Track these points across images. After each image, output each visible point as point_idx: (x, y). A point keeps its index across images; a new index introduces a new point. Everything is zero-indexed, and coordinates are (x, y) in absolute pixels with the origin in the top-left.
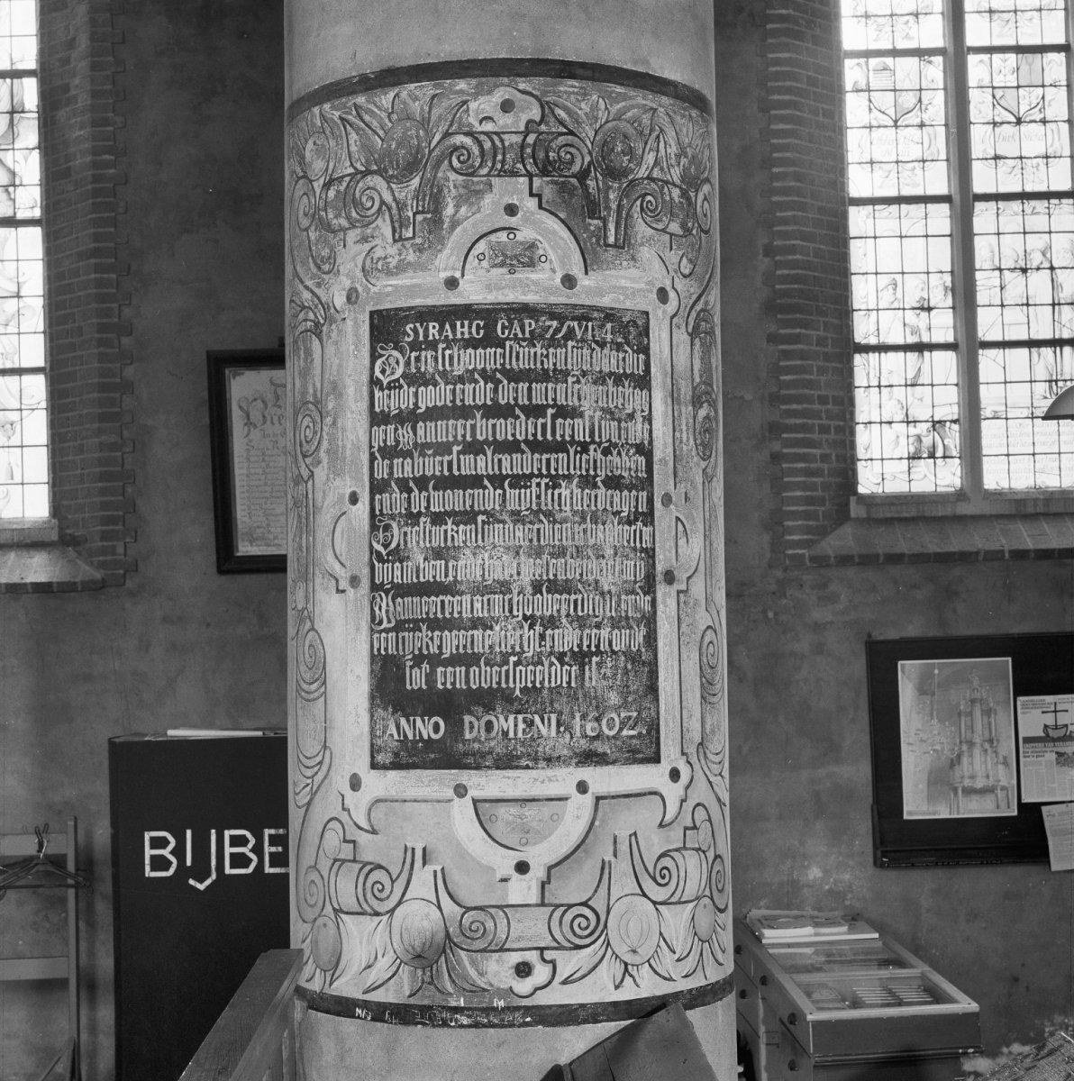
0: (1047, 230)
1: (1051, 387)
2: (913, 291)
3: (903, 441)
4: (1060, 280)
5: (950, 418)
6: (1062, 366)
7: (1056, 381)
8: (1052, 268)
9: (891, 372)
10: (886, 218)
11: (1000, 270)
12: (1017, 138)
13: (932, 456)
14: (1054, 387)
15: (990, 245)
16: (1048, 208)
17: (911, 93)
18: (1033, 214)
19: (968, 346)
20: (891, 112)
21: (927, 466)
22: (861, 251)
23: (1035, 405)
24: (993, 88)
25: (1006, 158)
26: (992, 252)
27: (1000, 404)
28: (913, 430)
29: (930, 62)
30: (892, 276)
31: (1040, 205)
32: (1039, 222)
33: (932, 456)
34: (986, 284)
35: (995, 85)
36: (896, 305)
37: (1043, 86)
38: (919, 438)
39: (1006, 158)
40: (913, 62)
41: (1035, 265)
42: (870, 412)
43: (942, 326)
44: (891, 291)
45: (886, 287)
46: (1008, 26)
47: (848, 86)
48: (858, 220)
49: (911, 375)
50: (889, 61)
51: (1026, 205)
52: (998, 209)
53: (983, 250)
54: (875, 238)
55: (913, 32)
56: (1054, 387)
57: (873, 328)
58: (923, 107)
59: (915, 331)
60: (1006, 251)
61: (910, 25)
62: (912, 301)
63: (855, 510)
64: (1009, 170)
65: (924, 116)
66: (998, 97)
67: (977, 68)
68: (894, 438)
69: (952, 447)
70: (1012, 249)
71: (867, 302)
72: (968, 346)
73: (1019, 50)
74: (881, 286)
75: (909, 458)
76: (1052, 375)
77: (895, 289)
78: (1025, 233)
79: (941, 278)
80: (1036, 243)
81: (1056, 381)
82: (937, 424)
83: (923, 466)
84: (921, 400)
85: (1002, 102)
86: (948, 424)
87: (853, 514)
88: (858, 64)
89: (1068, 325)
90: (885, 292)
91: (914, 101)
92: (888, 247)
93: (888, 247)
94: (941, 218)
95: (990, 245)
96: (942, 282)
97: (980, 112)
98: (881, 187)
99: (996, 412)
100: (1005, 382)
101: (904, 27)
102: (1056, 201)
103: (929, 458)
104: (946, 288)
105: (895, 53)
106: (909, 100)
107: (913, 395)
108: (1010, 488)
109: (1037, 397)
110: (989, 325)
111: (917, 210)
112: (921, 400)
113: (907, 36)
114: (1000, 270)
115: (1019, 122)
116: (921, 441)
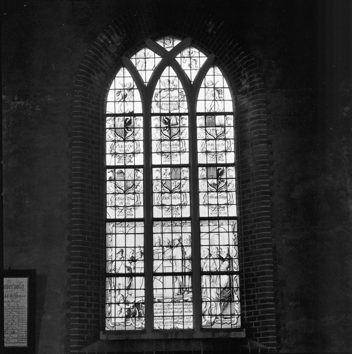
0: (181, 232)
1: (180, 291)
2: (129, 254)
3: (123, 310)
4: (185, 250)
5: (142, 302)
6: (185, 282)
7: (183, 288)
8: (182, 246)
9: (120, 284)
11: (163, 246)
12: (170, 198)
13: (134, 316)
14: (182, 291)
15: (159, 237)
16: (181, 224)
17: (131, 182)
18: (175, 226)
19: (149, 274)
20: (123, 188)
21: (132, 320)
22: (110, 239)
23: (174, 297)
24: (162, 180)
25: (166, 205)
26: (160, 240)
27: (161, 297)
28: (127, 307)
29: (139, 171)
31: (178, 223)
32: (178, 229)
33: (134, 316)
34: (157, 251)
35: (162, 179)
36: (122, 259)
37: (180, 179)
38: (129, 309)
39: (166, 205)
40: (132, 170)
41: (176, 244)
42: (111, 299)
43: (140, 267)
44: (121, 254)
45: (119, 252)
46: (168, 158)
47: (108, 179)
48: (110, 228)
49: (127, 285)
50: (123, 170)
51: (173, 223)
52: (162, 224)
53: (156, 238)
54: (116, 234)
55: (133, 160)
56: (182, 291)
57: (113, 268)
58: (135, 186)
59: (129, 269)
60: (165, 239)
61: (131, 157)
62: (128, 257)
63: (103, 337)
64: (167, 210)
65: (135, 190)
66: (163, 183)
67: (156, 173)
68: (120, 309)
69: (142, 313)
70: (167, 238)
72: (149, 274)
73: (172, 166)
74: (117, 252)
75: (125, 317)
76: (181, 286)
77: (122, 253)
78: (172, 233)
79: (140, 249)
80: (176, 236)
81: (183, 288)
82: (136, 305)
83: (130, 321)
84: (131, 295)
85: (165, 185)
86: (141, 304)
87: (101, 339)
88: (111, 171)
89: (188, 267)
90: (119, 254)
91: (132, 184)
94: (140, 228)
95: (159, 237)
96: (140, 251)
97: (157, 189)
98: (118, 215)
99: (159, 300)
100: (163, 289)
101: (129, 158)
102: (184, 221)
103: (133, 317)
104: (142, 253)
105: (125, 167)
106: (130, 184)
107: (128, 293)
108: (164, 329)
109: (175, 294)
110: (157, 266)
111: (132, 224)
112: (131, 295)
113: (130, 161)
114: (163, 246)
115: (171, 192)
116: (130, 311)
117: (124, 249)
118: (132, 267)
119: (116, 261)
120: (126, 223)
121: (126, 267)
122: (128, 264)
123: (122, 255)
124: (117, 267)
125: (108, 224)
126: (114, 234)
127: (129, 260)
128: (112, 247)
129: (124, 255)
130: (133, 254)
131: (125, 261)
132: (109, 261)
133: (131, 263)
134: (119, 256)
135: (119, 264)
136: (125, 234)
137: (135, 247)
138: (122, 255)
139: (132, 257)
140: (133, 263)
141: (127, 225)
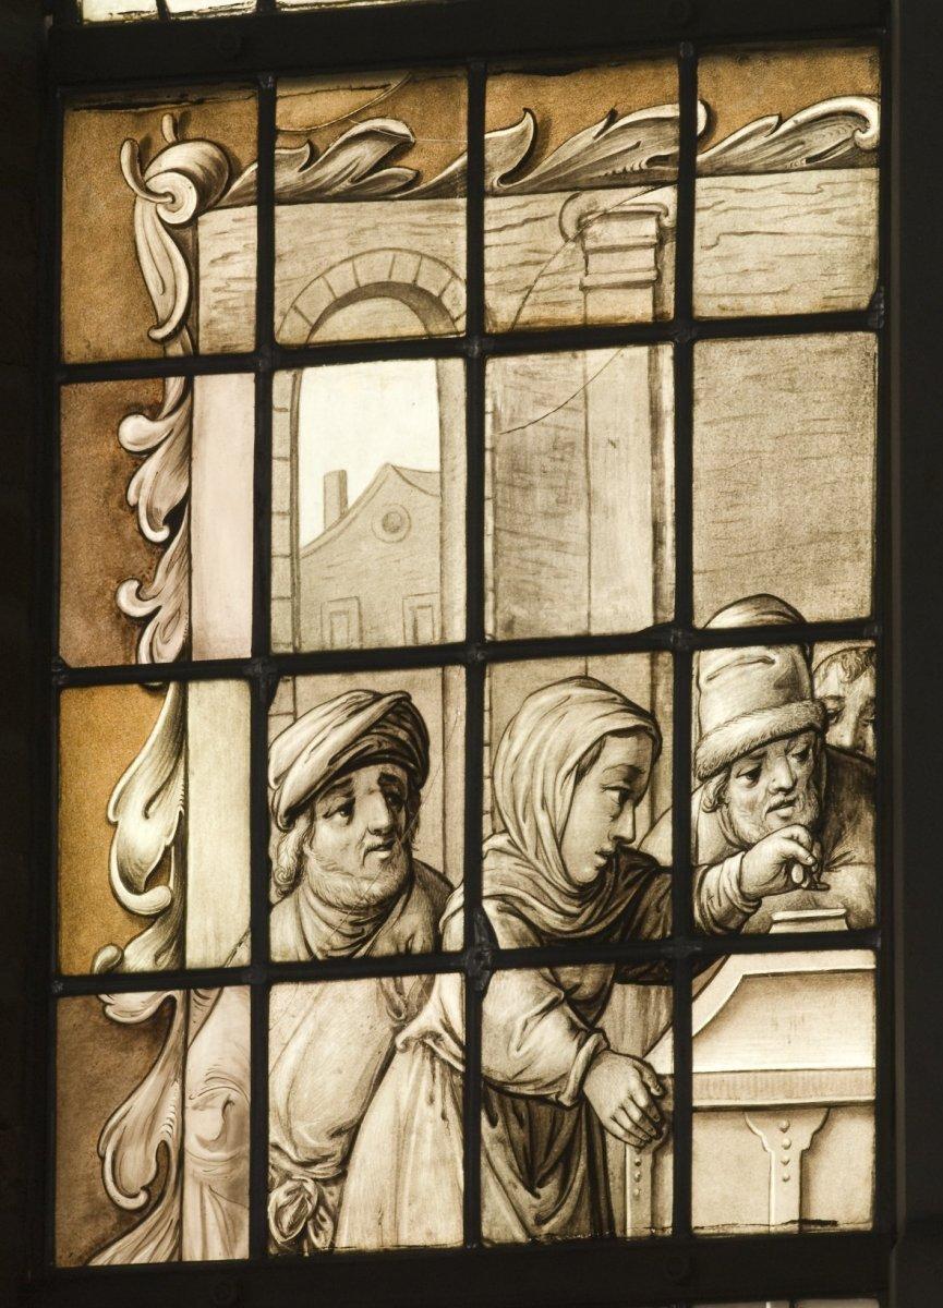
10: (359, 190)
30: (389, 681)
36: (410, 925)
44: (374, 812)
54: (271, 358)
62: (525, 881)
71: (173, 920)
77: (404, 799)
79: (792, 688)
90: (329, 833)
92: (373, 426)
93: (373, 426)
96: (798, 714)
104: (831, 782)
117: (437, 699)
118: (617, 1093)
119: (261, 974)
120: (501, 97)
121: (476, 1093)
122: (526, 1029)
123: (399, 836)
124: (301, 1125)
125: (93, 146)
126: (226, 362)
127: (541, 953)
128: (189, 669)
129: (437, 838)
130: (631, 787)
131: (479, 963)
132: (118, 979)
133: (585, 1015)
134: (342, 855)
135: (324, 1031)
136: (478, 343)
137: (677, 639)
138: (399, 836)
139: (624, 860)
140: (629, 1010)
141: (503, 147)
